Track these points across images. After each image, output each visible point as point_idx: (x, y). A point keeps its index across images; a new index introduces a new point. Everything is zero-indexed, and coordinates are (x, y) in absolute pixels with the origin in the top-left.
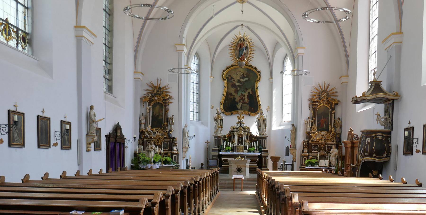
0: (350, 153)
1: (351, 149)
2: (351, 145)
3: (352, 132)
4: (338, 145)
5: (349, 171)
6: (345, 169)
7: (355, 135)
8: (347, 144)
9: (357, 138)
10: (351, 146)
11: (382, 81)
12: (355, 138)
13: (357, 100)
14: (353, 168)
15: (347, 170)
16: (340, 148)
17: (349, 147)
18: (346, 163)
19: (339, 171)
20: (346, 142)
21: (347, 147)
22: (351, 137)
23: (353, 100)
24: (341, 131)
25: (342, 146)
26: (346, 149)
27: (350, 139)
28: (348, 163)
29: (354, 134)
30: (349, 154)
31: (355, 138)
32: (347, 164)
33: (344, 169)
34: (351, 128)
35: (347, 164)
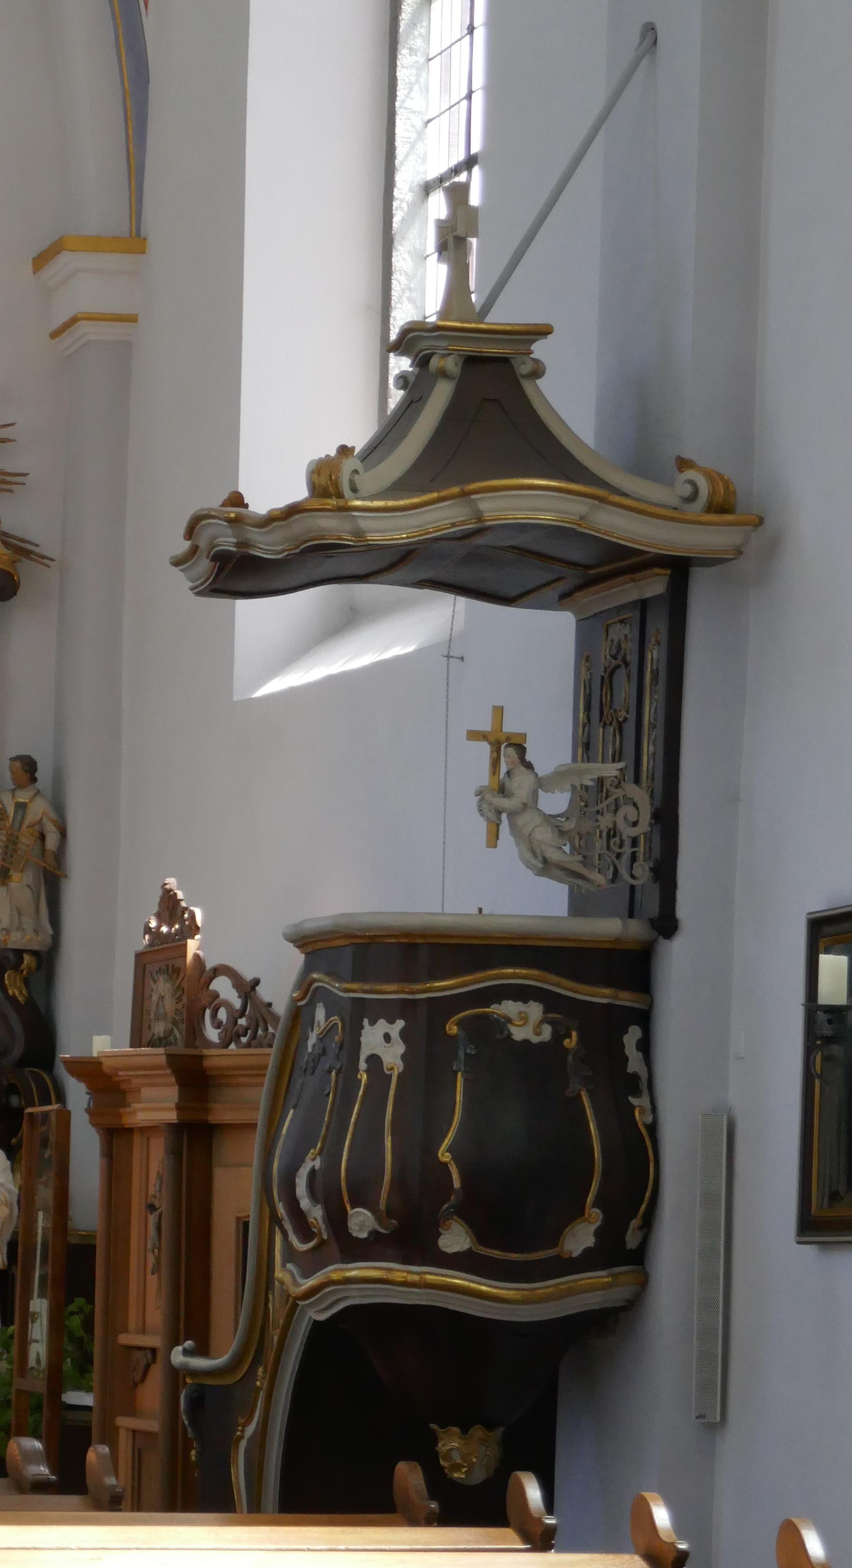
0: (164, 1205)
1: (175, 1153)
2: (179, 1108)
3: (193, 946)
4: (15, 1101)
5: (153, 1425)
6: (104, 1398)
7: (223, 986)
8: (124, 1092)
9: (242, 1022)
10: (172, 1116)
11: (543, 331)
12: (222, 1014)
13: (243, 544)
14: (197, 1402)
15: (123, 1422)
16: (45, 1143)
17: (148, 1130)
18: (111, 1332)
19: (21, 1433)
20: (107, 1063)
21: (130, 1131)
22: (169, 1004)
23: (203, 543)
24: (50, 931)
25: (65, 1117)
26: (108, 1153)
27: (159, 1028)
28: (132, 1323)
29: (217, 971)
30: (152, 1219)
31: (222, 1014)
32: (131, 1348)
33: (86, 1399)
34: (180, 895)
35: (124, 1339)
